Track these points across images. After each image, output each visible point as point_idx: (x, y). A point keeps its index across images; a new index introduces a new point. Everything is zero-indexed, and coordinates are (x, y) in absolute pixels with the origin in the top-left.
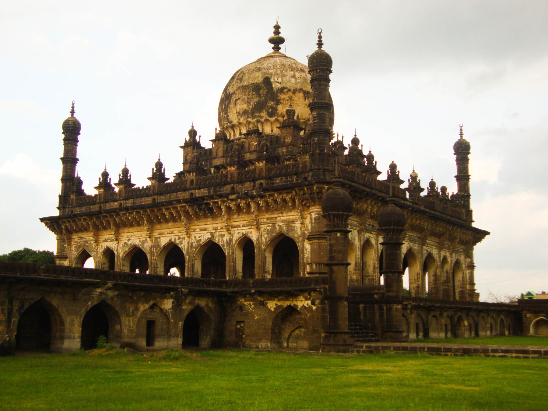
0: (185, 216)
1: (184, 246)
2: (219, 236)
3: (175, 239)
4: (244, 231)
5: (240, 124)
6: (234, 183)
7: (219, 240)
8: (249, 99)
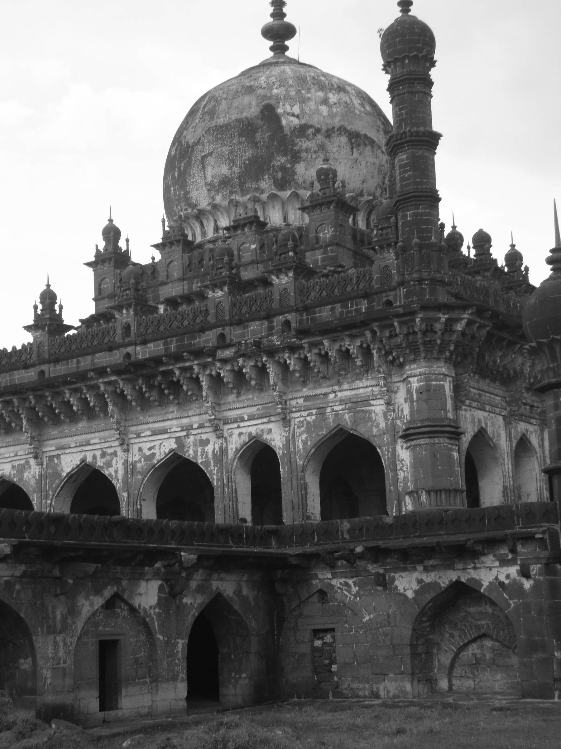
0: (115, 404)
1: (116, 471)
2: (195, 444)
3: (94, 457)
4: (252, 428)
5: (215, 207)
6: (224, 325)
7: (196, 452)
8: (231, 152)
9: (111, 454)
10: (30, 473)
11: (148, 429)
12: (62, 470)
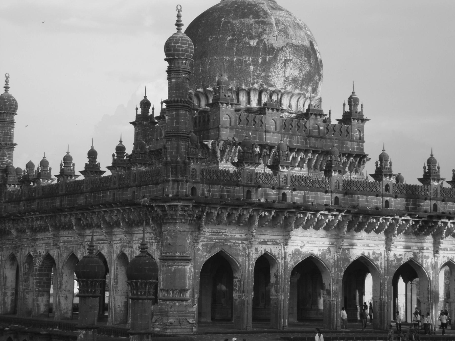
1: (381, 264)
3: (369, 254)
6: (437, 200)
9: (378, 254)
10: (330, 255)
11: (401, 245)
12: (351, 257)
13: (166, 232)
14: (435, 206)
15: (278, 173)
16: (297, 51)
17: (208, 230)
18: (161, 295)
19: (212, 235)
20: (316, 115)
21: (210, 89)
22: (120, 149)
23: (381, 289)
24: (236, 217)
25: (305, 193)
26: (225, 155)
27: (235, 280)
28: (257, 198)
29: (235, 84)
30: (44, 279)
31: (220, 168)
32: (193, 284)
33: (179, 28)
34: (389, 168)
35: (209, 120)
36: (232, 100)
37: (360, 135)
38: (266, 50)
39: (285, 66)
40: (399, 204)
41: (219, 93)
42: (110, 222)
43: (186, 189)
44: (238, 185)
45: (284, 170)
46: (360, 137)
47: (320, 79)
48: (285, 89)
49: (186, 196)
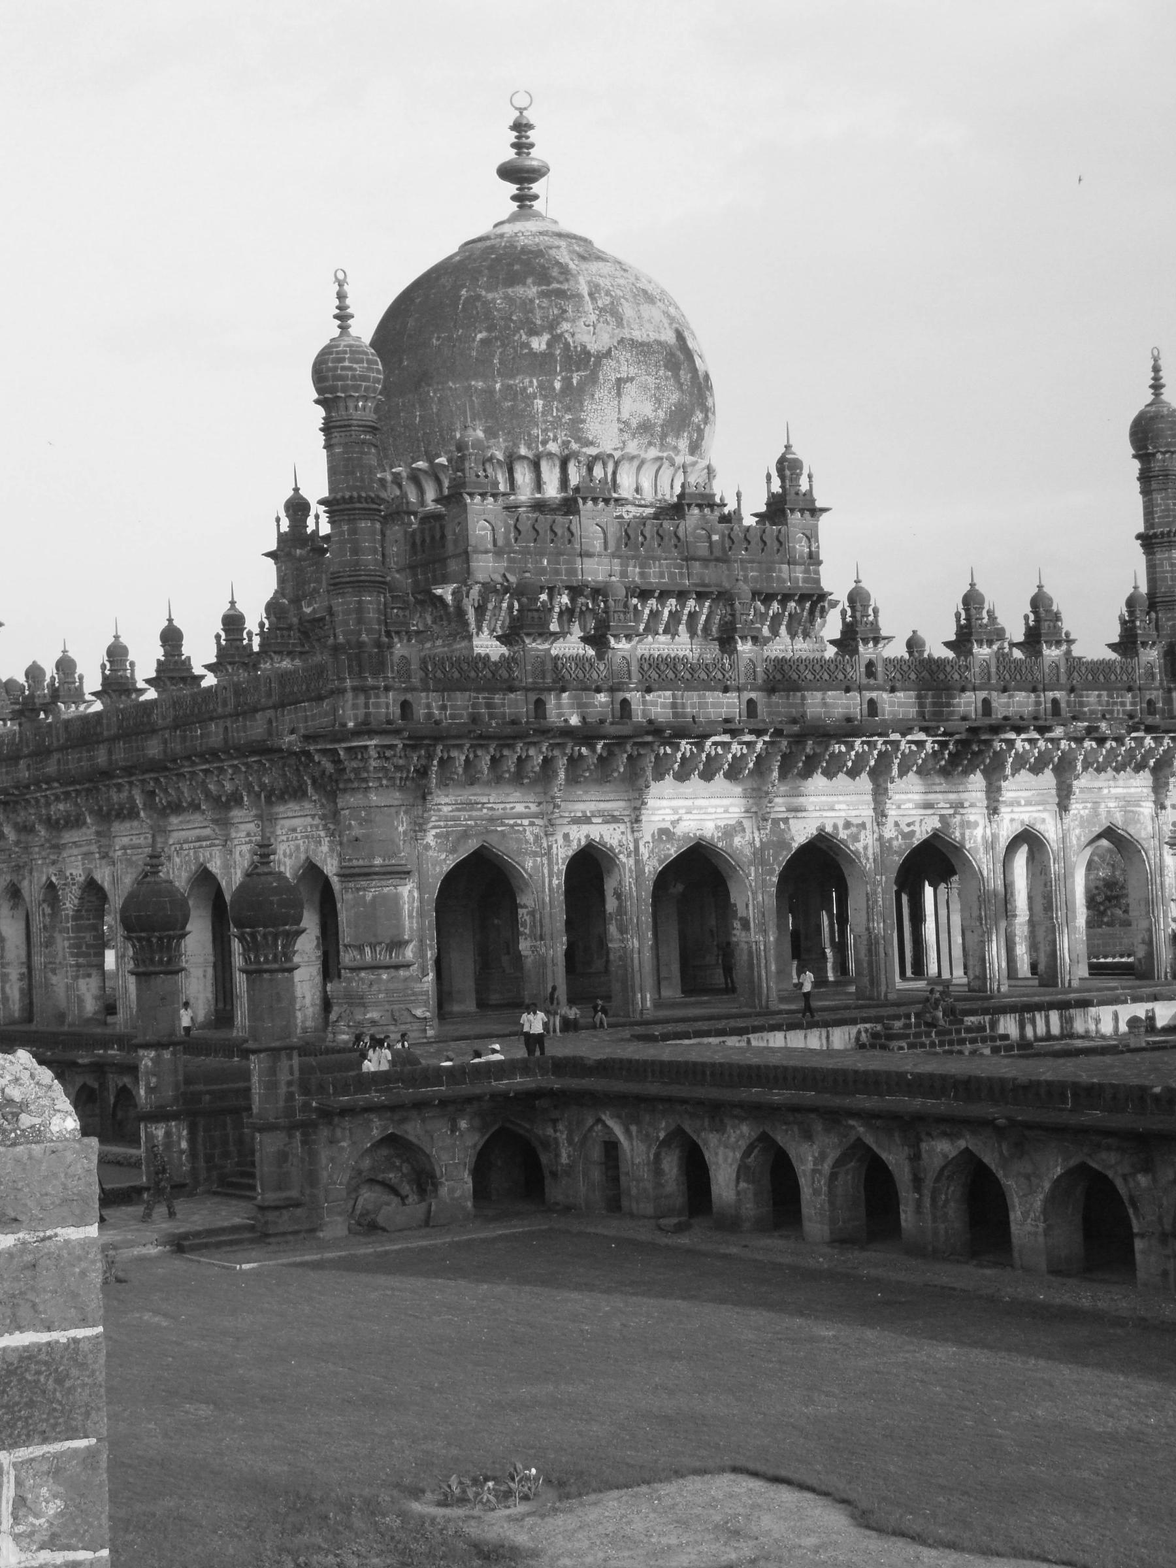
1: (866, 848)
3: (835, 827)
6: (990, 690)
9: (858, 826)
11: (909, 801)
13: (347, 812)
14: (986, 703)
15: (605, 652)
16: (645, 356)
17: (447, 800)
18: (347, 957)
19: (458, 810)
20: (699, 506)
21: (443, 460)
22: (233, 622)
23: (868, 907)
24: (510, 764)
25: (674, 697)
26: (487, 618)
27: (521, 911)
28: (560, 715)
29: (503, 445)
30: (89, 937)
31: (477, 650)
32: (421, 928)
33: (345, 324)
34: (872, 623)
35: (443, 536)
36: (496, 484)
37: (810, 547)
38: (570, 357)
39: (619, 394)
40: (900, 705)
41: (463, 471)
42: (220, 796)
43: (388, 705)
44: (512, 689)
45: (620, 646)
46: (810, 553)
47: (706, 420)
48: (622, 449)
49: (389, 722)
